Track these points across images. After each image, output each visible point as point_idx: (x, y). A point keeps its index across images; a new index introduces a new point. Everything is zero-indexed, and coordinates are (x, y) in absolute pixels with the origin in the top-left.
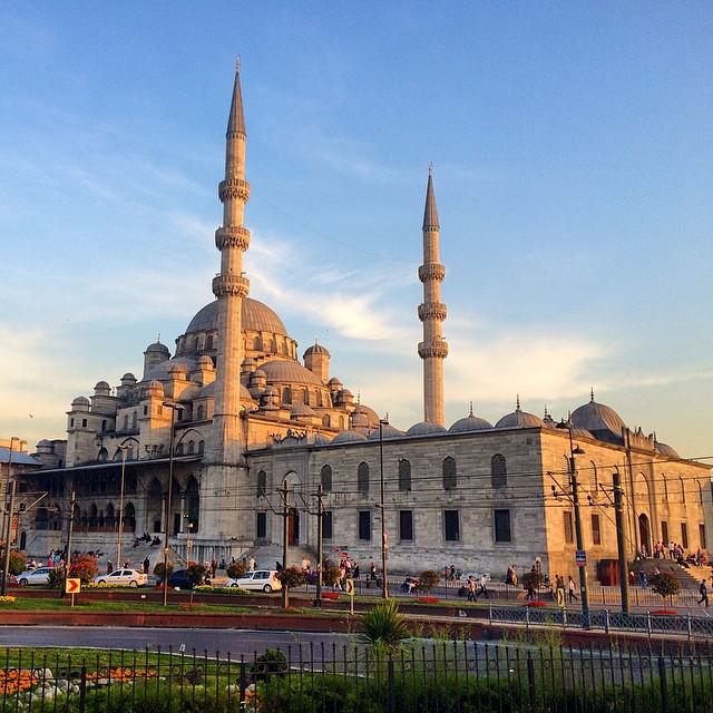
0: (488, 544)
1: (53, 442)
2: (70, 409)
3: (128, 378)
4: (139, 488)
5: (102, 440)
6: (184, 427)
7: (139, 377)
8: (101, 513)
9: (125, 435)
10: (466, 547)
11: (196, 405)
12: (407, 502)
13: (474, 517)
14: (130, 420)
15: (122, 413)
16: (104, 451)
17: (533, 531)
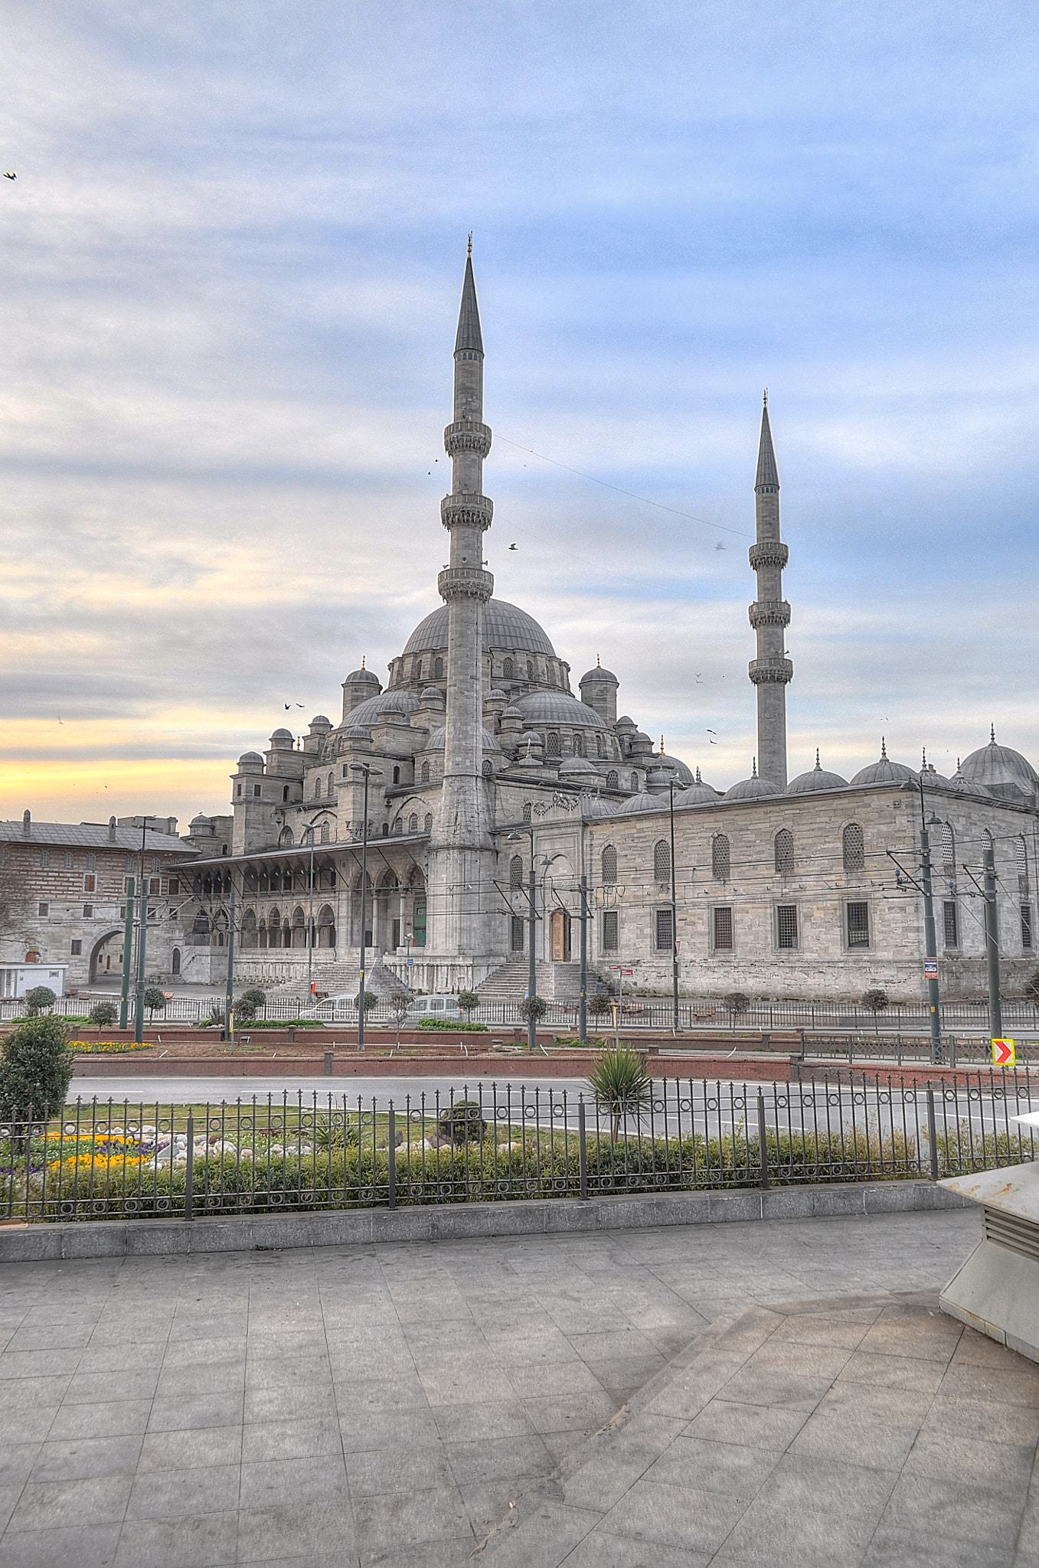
0: (837, 952)
1: (213, 819)
2: (236, 770)
3: (320, 725)
4: (340, 884)
5: (283, 813)
6: (403, 794)
7: (336, 720)
8: (286, 920)
9: (318, 807)
10: (807, 956)
11: (419, 761)
12: (725, 896)
13: (818, 915)
14: (324, 786)
15: (312, 774)
16: (287, 830)
17: (900, 931)
